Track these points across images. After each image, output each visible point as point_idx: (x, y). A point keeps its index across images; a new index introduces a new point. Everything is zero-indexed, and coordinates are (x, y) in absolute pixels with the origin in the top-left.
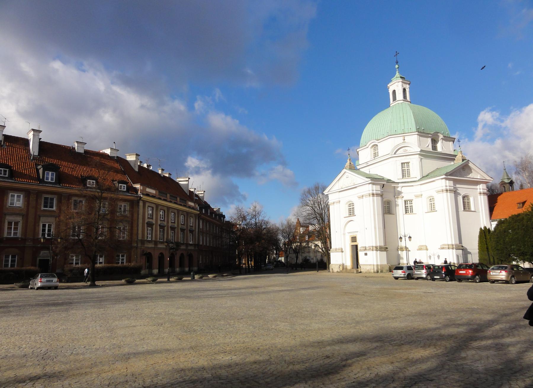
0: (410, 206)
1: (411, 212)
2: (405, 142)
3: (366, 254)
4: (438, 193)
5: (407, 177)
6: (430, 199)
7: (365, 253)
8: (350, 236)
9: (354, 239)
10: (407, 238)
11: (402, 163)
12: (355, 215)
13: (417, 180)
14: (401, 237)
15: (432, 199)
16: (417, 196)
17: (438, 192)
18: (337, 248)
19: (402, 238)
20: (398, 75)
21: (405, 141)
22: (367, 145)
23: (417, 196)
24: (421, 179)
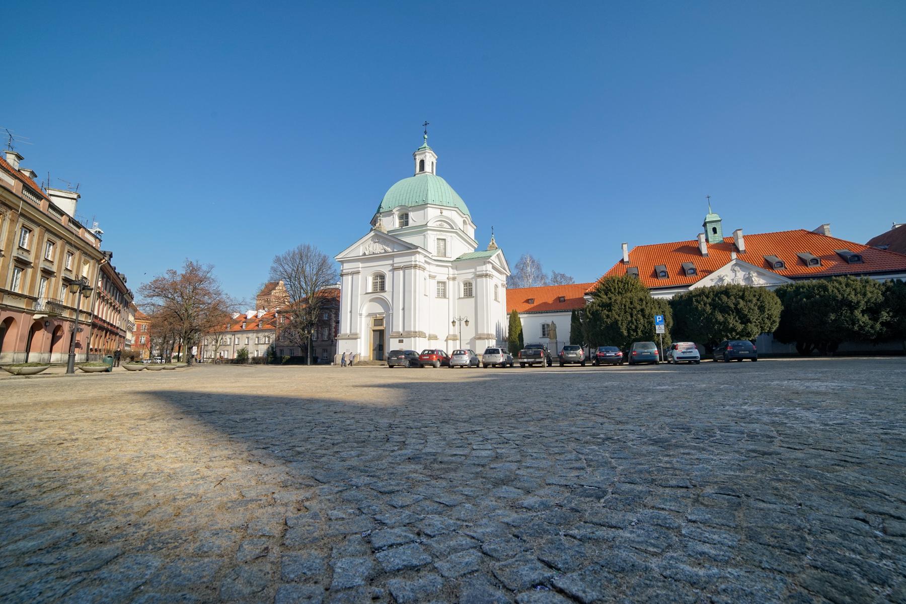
3: (401, 341)
9: (378, 321)
10: (463, 323)
20: (425, 145)
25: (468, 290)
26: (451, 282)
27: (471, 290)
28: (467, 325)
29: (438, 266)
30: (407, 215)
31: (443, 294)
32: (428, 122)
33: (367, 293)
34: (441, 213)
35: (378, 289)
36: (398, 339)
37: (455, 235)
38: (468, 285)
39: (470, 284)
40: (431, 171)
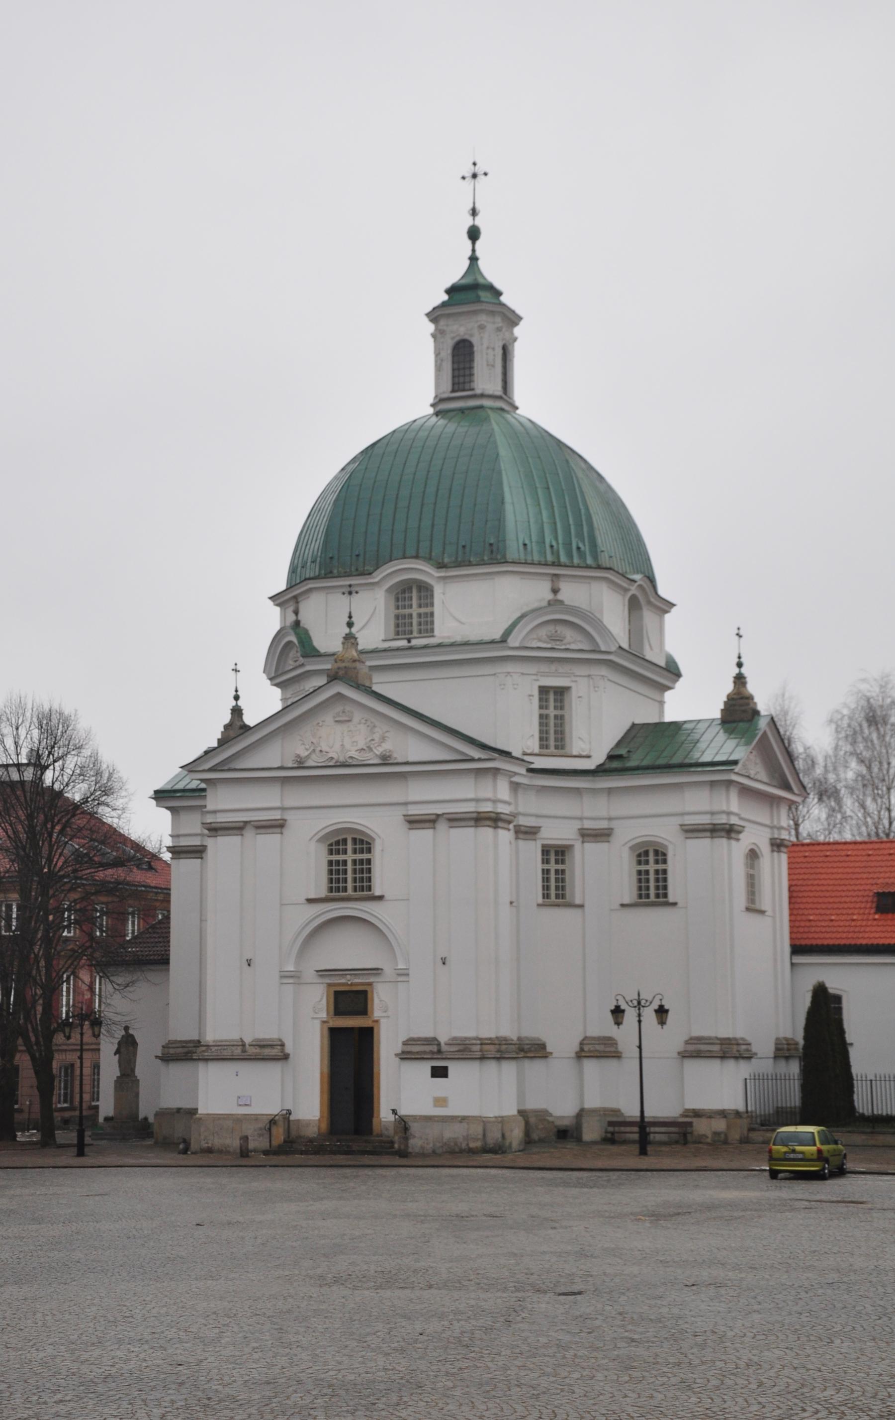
0: (557, 871)
1: (557, 896)
2: (561, 602)
3: (440, 1072)
5: (552, 750)
6: (642, 850)
7: (433, 1068)
8: (329, 985)
10: (649, 1014)
11: (544, 691)
12: (380, 898)
13: (593, 767)
15: (651, 854)
16: (588, 835)
17: (691, 831)
18: (248, 1040)
19: (623, 1011)
21: (560, 596)
22: (378, 576)
23: (588, 835)
24: (600, 771)
25: (652, 877)
27: (662, 876)
28: (662, 1022)
30: (425, 590)
32: (480, 169)
33: (310, 901)
34: (555, 591)
35: (350, 885)
36: (425, 1068)
37: (604, 671)
38: (651, 858)
39: (661, 856)
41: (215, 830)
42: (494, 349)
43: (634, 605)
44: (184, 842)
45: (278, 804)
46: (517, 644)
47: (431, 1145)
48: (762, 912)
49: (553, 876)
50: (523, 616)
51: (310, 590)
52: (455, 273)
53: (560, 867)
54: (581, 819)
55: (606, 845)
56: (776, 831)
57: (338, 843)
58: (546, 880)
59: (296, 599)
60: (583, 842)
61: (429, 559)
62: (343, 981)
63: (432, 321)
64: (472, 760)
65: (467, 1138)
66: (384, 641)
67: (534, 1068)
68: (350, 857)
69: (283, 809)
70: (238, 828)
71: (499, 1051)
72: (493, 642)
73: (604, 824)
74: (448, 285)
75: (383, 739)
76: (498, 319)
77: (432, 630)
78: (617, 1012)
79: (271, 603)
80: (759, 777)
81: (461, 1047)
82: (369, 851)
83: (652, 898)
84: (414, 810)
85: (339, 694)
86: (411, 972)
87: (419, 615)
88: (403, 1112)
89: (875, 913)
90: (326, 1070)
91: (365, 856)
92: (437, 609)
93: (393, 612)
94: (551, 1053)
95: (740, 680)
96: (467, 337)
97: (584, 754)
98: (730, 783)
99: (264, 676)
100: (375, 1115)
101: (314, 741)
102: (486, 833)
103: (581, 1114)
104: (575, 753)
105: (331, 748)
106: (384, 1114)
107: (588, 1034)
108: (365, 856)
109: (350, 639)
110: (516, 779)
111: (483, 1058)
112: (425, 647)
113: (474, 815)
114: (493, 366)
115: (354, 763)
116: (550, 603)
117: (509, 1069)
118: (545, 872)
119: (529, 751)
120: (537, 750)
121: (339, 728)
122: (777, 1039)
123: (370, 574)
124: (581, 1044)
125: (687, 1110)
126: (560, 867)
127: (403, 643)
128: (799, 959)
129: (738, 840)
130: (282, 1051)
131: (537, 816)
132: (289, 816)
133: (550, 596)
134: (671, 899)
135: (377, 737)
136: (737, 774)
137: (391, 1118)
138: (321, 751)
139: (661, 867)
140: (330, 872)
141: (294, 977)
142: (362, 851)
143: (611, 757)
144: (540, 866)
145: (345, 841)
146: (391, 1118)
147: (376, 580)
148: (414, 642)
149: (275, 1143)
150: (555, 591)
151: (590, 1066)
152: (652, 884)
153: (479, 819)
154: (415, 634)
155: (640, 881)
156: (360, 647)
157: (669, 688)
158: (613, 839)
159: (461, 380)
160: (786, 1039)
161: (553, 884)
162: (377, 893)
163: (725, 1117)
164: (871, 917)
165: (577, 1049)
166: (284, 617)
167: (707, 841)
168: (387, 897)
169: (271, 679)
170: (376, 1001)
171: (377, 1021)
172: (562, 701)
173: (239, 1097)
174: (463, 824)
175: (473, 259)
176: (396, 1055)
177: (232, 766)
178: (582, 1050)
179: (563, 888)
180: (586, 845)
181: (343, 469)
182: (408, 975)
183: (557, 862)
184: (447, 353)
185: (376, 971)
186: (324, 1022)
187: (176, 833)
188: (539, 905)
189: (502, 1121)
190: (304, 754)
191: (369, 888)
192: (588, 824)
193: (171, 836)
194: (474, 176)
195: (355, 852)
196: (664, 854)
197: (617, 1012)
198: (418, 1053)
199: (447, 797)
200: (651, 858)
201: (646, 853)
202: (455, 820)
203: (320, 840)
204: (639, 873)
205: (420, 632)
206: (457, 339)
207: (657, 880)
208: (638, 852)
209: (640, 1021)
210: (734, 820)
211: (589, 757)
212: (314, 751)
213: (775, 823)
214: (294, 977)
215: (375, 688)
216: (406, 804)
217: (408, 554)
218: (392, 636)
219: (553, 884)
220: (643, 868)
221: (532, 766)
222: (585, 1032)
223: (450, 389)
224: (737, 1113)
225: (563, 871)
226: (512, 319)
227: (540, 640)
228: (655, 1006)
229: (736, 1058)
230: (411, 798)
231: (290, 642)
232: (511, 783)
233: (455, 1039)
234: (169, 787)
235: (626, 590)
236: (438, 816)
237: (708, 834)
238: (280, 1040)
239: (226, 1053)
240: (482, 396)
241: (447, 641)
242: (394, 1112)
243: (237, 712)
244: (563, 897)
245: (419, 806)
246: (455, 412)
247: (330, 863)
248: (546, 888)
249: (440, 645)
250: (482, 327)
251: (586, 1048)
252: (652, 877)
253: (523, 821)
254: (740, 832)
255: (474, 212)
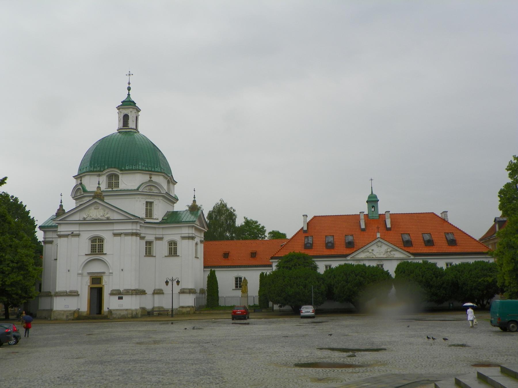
0: (149, 248)
2: (152, 181)
3: (120, 298)
4: (183, 239)
5: (149, 217)
8: (91, 276)
10: (175, 283)
11: (147, 202)
12: (106, 254)
14: (167, 281)
17: (183, 238)
18: (68, 291)
21: (152, 179)
22: (104, 172)
23: (157, 239)
25: (173, 249)
26: (159, 242)
27: (176, 249)
29: (146, 227)
30: (117, 177)
31: (149, 253)
32: (131, 73)
33: (86, 255)
34: (151, 178)
35: (97, 251)
36: (117, 297)
38: (173, 244)
39: (175, 243)
40: (135, 128)
41: (60, 236)
42: (134, 117)
43: (168, 182)
44: (47, 240)
45: (78, 230)
46: (141, 191)
47: (118, 316)
48: (198, 258)
49: (148, 249)
50: (142, 184)
51: (86, 175)
52: (124, 97)
53: (150, 247)
54: (155, 235)
55: (162, 241)
56: (201, 238)
57: (94, 240)
58: (146, 250)
59: (81, 177)
60: (156, 240)
61: (118, 168)
62: (94, 275)
63: (118, 109)
64: (131, 219)
65: (127, 314)
66: (105, 189)
67: (143, 297)
68: (97, 244)
69: (79, 231)
70: (66, 236)
71: (136, 292)
72: (135, 190)
73: (161, 236)
74: (122, 100)
75: (107, 213)
76: (135, 110)
77: (119, 187)
78: (167, 283)
79: (73, 178)
80: (199, 225)
81: (126, 292)
82: (103, 242)
83: (173, 254)
84: (115, 232)
85: (96, 202)
86: (113, 273)
87: (115, 183)
88: (110, 308)
89: (223, 258)
90: (89, 298)
91: (101, 243)
92: (120, 181)
93: (108, 181)
94: (147, 293)
95: (194, 201)
96: (127, 114)
97: (157, 218)
98: (193, 226)
99: (71, 197)
100: (102, 309)
101: (88, 213)
102: (134, 238)
103: (153, 308)
104: (154, 218)
105: (93, 215)
106: (105, 309)
107: (156, 288)
108: (101, 243)
109: (99, 188)
110: (141, 225)
111: (132, 294)
112: (117, 190)
113: (131, 233)
114: (134, 121)
115: (99, 219)
116: (149, 181)
117: (138, 297)
118: (146, 248)
119: (143, 217)
120: (145, 217)
121: (95, 210)
122: (200, 289)
123: (102, 171)
124: (154, 291)
125: (180, 306)
126: (150, 247)
127: (111, 189)
128: (205, 269)
129: (194, 240)
130: (77, 293)
131: (145, 234)
132: (81, 233)
133: (149, 179)
134: (178, 255)
135: (106, 213)
136: (195, 224)
137: (107, 310)
138: (90, 216)
139: (175, 247)
140: (92, 247)
141: (81, 274)
142: (101, 242)
143: (163, 219)
144: (145, 246)
145: (96, 240)
146: (107, 310)
147: (104, 173)
148: (113, 189)
149: (75, 316)
150: (151, 178)
151: (156, 296)
152: (173, 251)
153: (132, 234)
154: (114, 187)
155: (170, 250)
156: (101, 190)
157: (176, 203)
158: (163, 240)
159: (125, 124)
160: (202, 288)
161: (148, 251)
162: (105, 253)
163: (190, 308)
164: (222, 259)
165: (153, 292)
166: (77, 182)
167: (187, 240)
168: (107, 253)
169: (73, 198)
170: (103, 280)
171: (103, 286)
172: (151, 205)
173: (65, 306)
174: (129, 235)
175: (129, 95)
176: (109, 294)
177: (66, 220)
178: (154, 292)
179: (150, 252)
180: (156, 241)
181: (94, 145)
182: (112, 274)
183: (149, 245)
184: (122, 117)
185: (104, 273)
186: (89, 286)
187: (45, 237)
188: (144, 256)
189: (136, 310)
190: (85, 217)
191: (102, 252)
192: (157, 236)
193: (43, 238)
194: (129, 75)
195: (99, 242)
196: (176, 244)
197: (167, 283)
198: (115, 293)
199: (118, 229)
200: (173, 244)
201: (172, 243)
202: (126, 234)
203: (90, 239)
204: (170, 248)
205: (115, 187)
206: (125, 114)
207: (174, 250)
208: (170, 243)
209: (172, 284)
210: (194, 235)
211: (158, 219)
212: (88, 216)
213: (201, 236)
214: (81, 274)
215: (105, 201)
216: (113, 230)
217: (112, 166)
218: (107, 188)
219: (148, 251)
220: (171, 247)
221: (146, 221)
222: (155, 288)
223: (122, 126)
224: (192, 307)
225: (151, 248)
226: (138, 110)
227: (146, 190)
228: (176, 280)
229: (193, 293)
230: (115, 229)
231: (79, 188)
232: (140, 225)
233: (125, 289)
234: (43, 225)
235: (167, 178)
236: (122, 233)
237: (187, 239)
238: (77, 291)
239: (62, 294)
240: (131, 129)
241: (122, 189)
242: (108, 308)
243: (61, 206)
244: (150, 254)
245: (129, 230)
246: (123, 132)
247: (92, 245)
248: (146, 252)
249: (121, 190)
250: (131, 112)
251: (155, 292)
252: (173, 249)
253: (142, 235)
254: (195, 238)
255: (129, 84)
